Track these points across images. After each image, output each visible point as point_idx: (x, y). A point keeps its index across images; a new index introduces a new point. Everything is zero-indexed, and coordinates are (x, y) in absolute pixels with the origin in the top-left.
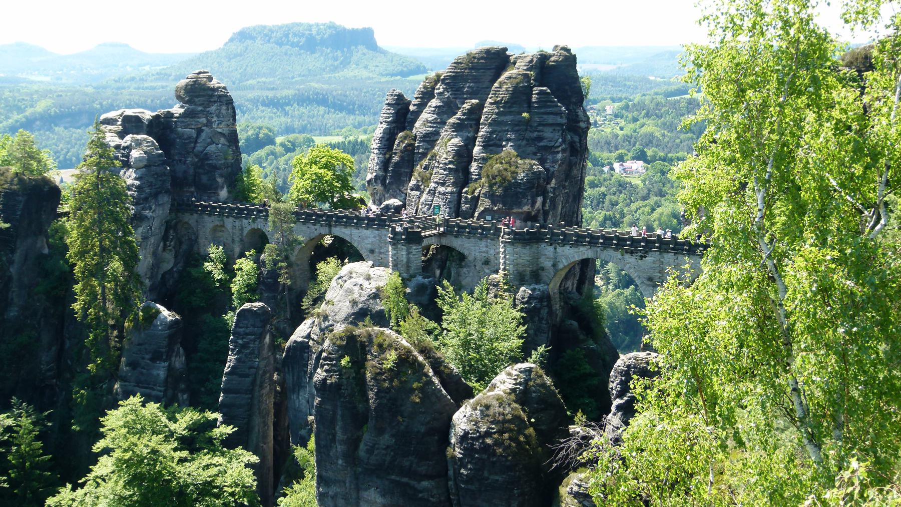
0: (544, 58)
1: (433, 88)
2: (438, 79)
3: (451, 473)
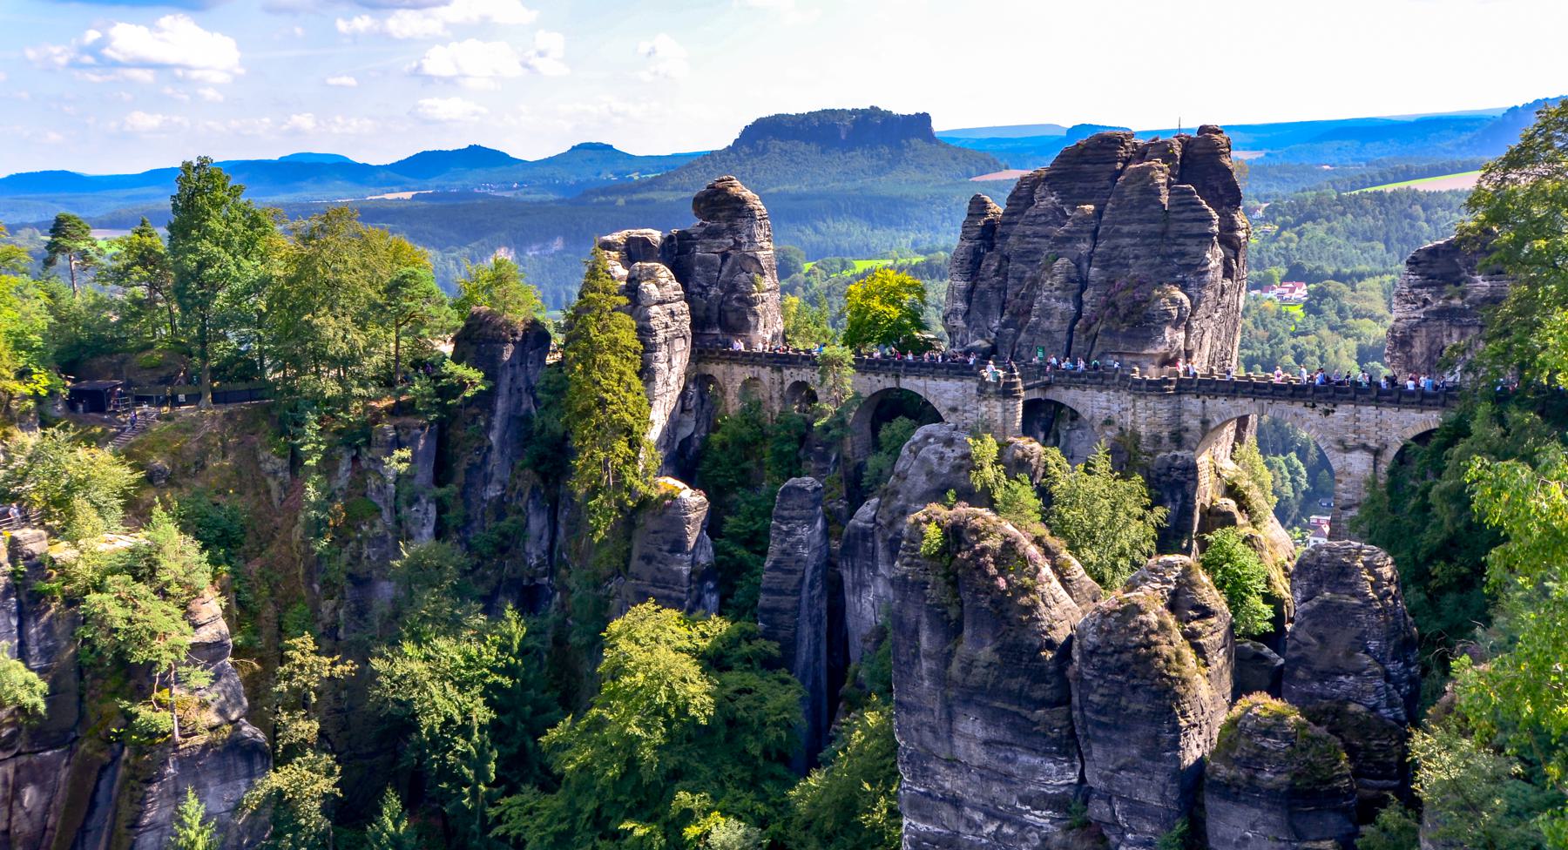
0: (1187, 144)
1: (1032, 191)
3: (1075, 700)
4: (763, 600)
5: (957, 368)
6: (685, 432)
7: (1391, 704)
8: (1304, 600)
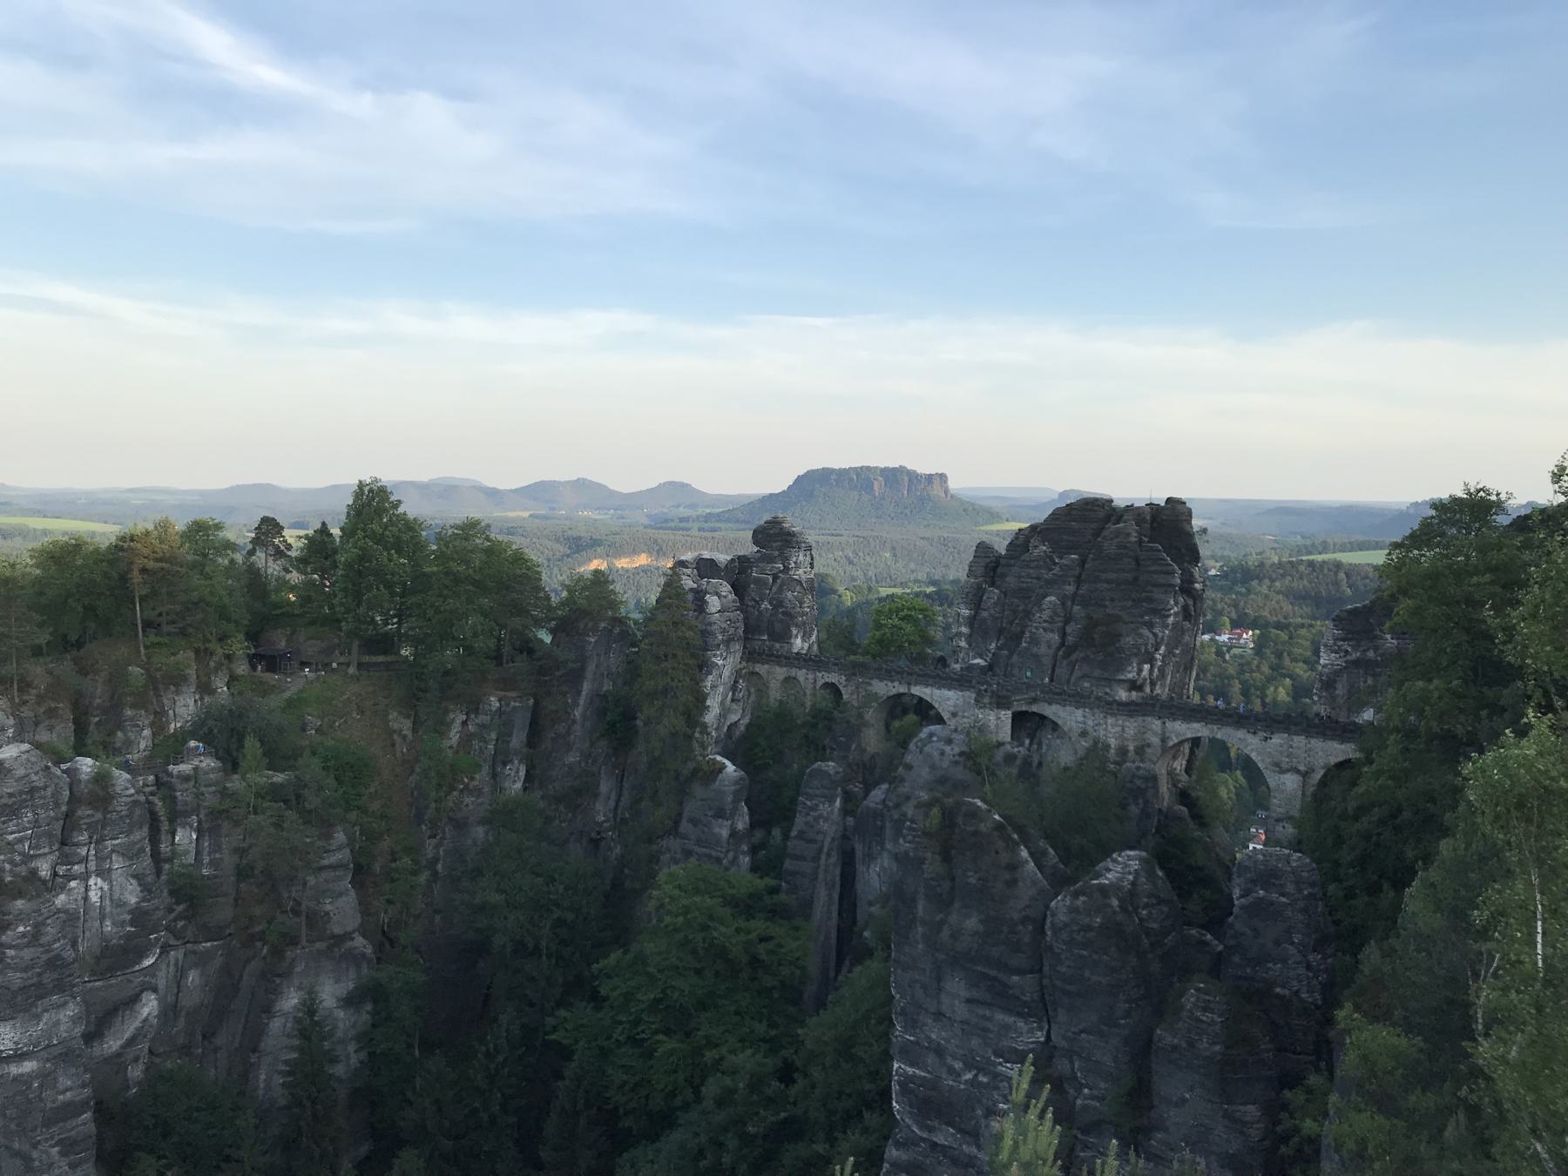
2: (1033, 528)
4: (788, 864)
5: (960, 682)
6: (733, 718)
7: (1310, 992)
8: (1242, 896)
